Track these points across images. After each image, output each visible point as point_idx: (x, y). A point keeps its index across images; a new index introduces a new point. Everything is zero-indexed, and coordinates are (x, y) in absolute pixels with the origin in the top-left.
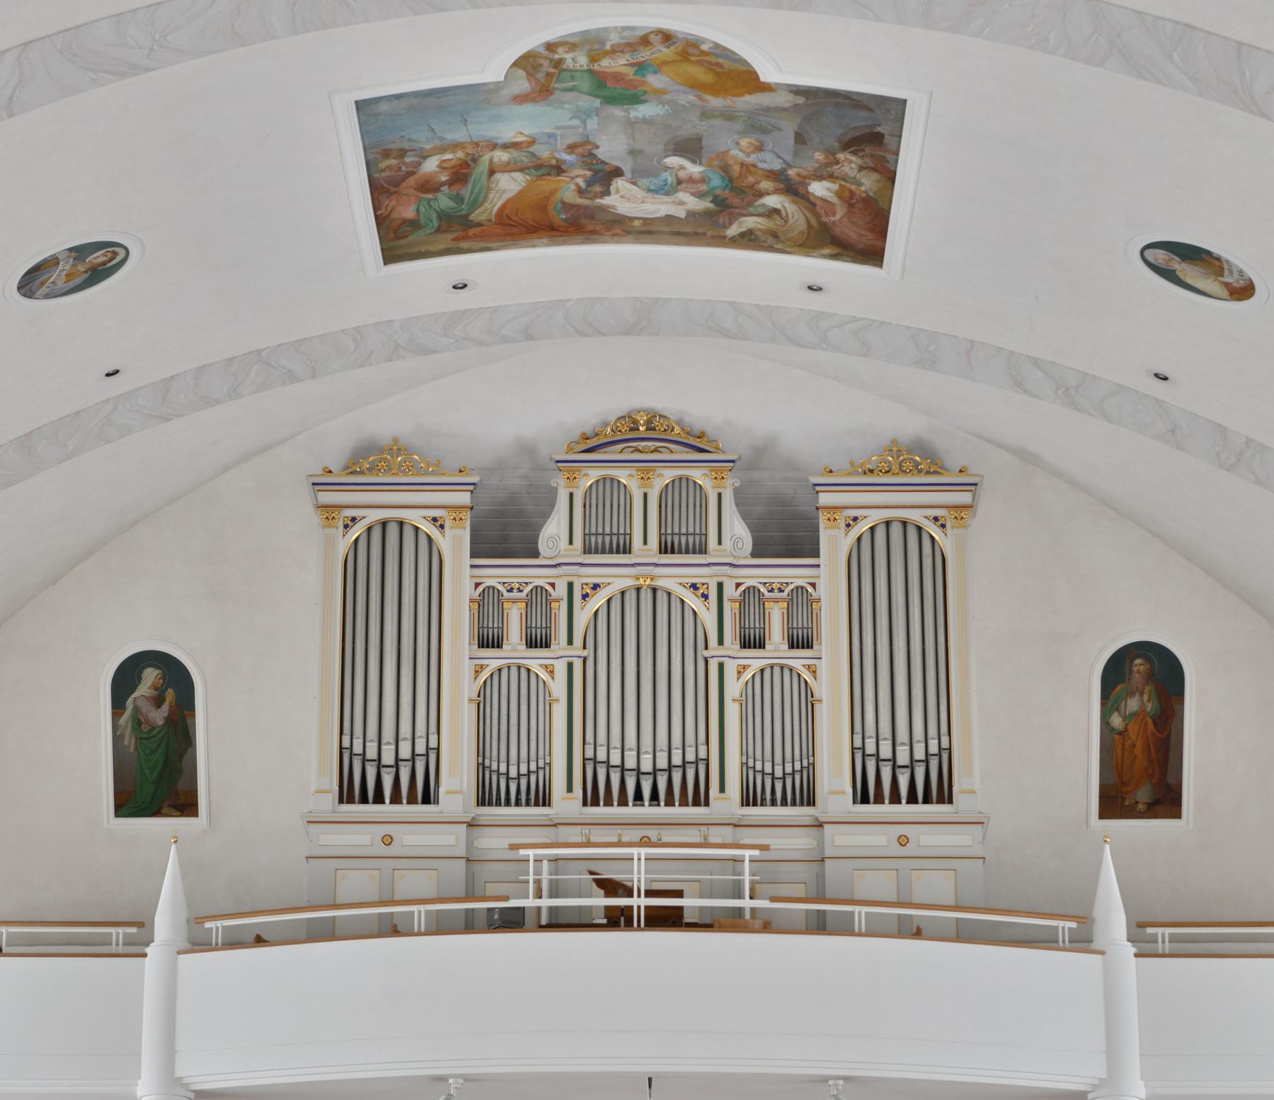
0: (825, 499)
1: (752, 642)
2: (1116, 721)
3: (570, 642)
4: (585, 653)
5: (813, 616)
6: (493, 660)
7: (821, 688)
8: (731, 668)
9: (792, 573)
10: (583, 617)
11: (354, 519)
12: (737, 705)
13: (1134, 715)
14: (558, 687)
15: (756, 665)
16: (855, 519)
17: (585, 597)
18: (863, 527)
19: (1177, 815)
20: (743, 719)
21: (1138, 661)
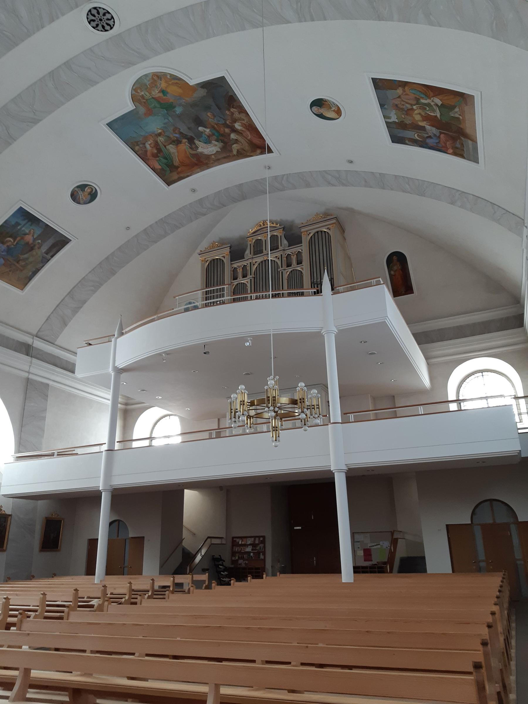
0: (303, 230)
1: (289, 265)
2: (392, 273)
3: (251, 275)
4: (254, 276)
5: (301, 256)
6: (236, 282)
7: (304, 272)
8: (284, 272)
9: (296, 249)
10: (254, 268)
11: (208, 260)
12: (286, 280)
13: (396, 270)
14: (249, 285)
15: (290, 270)
16: (310, 233)
17: (254, 265)
18: (311, 235)
19: (413, 293)
20: (288, 282)
21: (394, 257)
